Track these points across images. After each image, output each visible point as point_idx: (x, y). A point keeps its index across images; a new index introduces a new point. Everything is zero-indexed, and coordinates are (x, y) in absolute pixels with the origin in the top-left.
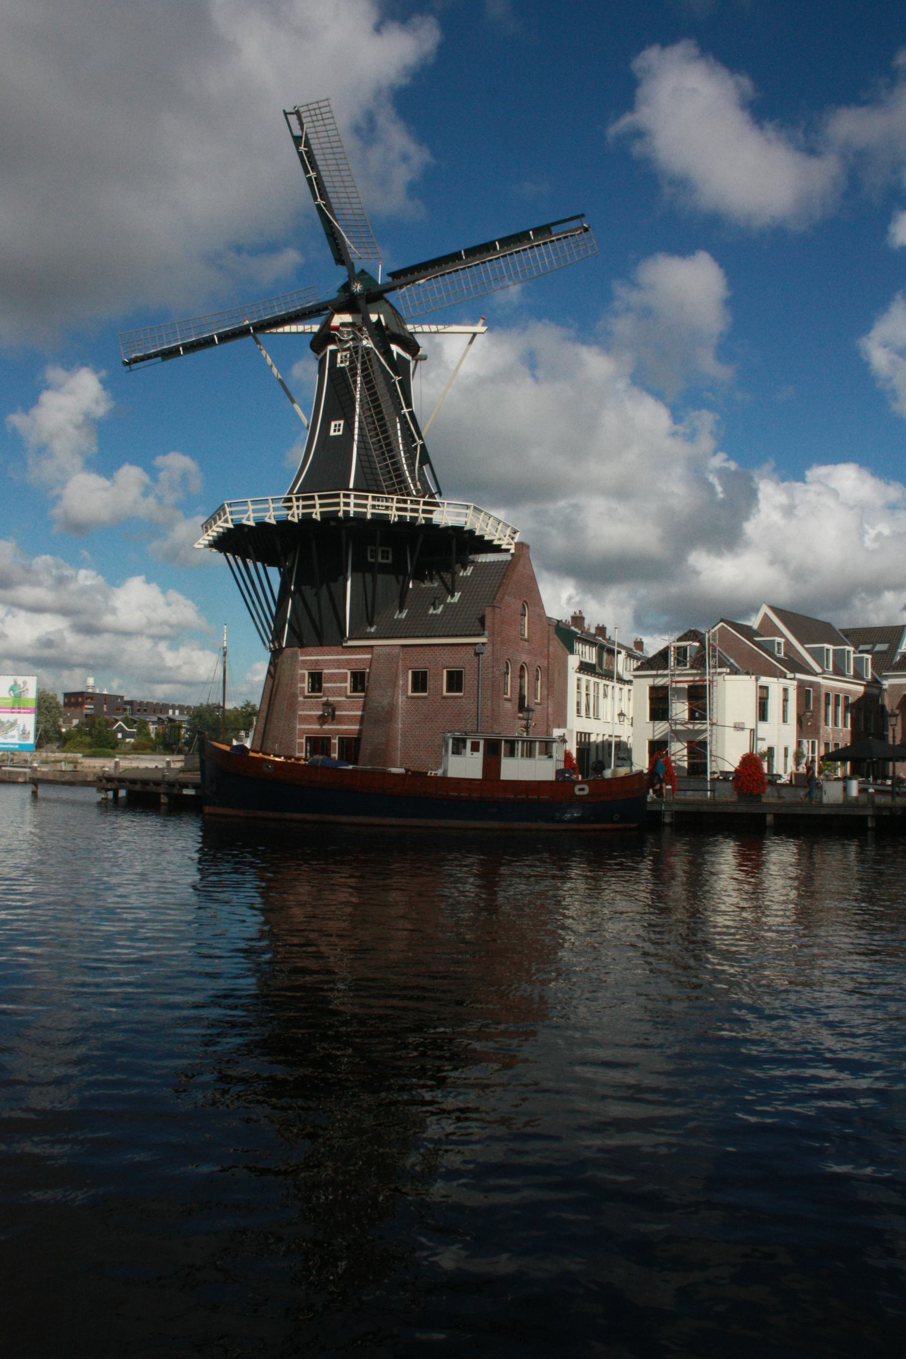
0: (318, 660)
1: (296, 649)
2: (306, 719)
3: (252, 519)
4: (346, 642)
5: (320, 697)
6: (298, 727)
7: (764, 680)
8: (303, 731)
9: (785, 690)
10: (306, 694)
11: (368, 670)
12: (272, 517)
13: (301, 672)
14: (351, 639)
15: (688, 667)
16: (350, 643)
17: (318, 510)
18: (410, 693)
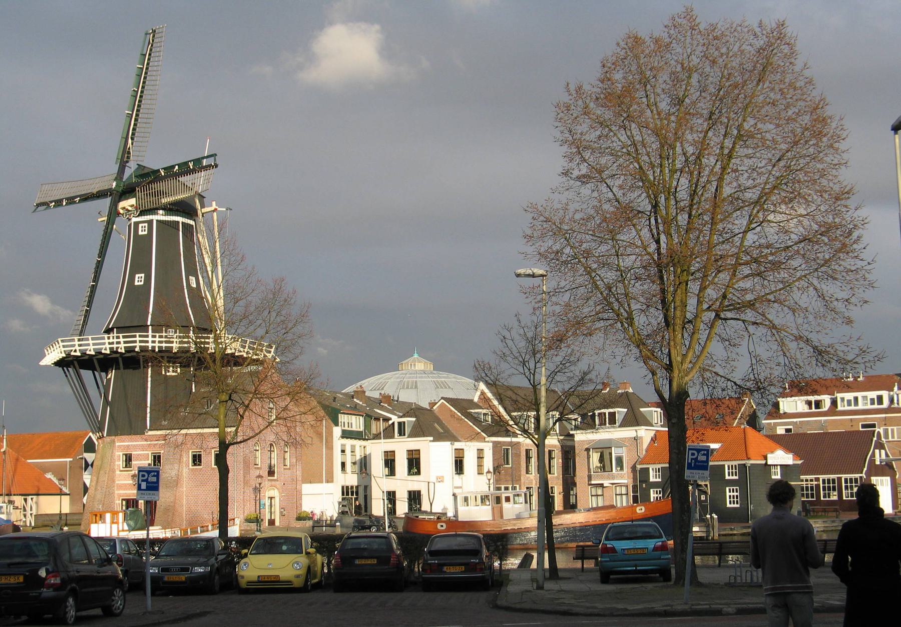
0: (129, 445)
1: (113, 437)
2: (121, 487)
3: (78, 351)
4: (147, 432)
5: (131, 471)
6: (116, 492)
7: (458, 445)
8: (120, 495)
9: (480, 451)
10: (122, 469)
11: (162, 452)
12: (92, 350)
13: (117, 453)
14: (150, 430)
15: (406, 436)
16: (150, 433)
17: (122, 345)
18: (191, 467)
